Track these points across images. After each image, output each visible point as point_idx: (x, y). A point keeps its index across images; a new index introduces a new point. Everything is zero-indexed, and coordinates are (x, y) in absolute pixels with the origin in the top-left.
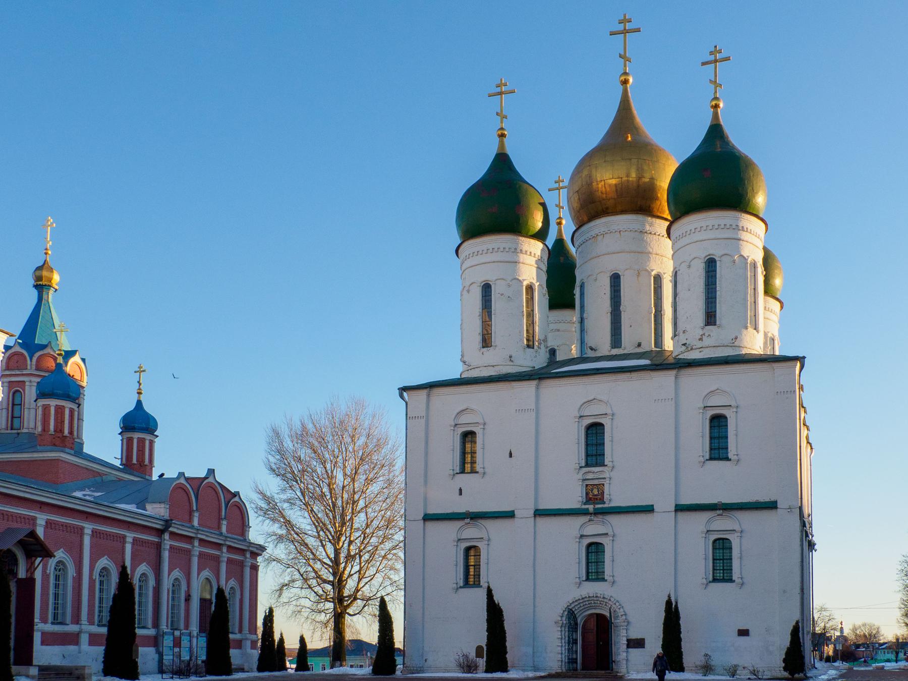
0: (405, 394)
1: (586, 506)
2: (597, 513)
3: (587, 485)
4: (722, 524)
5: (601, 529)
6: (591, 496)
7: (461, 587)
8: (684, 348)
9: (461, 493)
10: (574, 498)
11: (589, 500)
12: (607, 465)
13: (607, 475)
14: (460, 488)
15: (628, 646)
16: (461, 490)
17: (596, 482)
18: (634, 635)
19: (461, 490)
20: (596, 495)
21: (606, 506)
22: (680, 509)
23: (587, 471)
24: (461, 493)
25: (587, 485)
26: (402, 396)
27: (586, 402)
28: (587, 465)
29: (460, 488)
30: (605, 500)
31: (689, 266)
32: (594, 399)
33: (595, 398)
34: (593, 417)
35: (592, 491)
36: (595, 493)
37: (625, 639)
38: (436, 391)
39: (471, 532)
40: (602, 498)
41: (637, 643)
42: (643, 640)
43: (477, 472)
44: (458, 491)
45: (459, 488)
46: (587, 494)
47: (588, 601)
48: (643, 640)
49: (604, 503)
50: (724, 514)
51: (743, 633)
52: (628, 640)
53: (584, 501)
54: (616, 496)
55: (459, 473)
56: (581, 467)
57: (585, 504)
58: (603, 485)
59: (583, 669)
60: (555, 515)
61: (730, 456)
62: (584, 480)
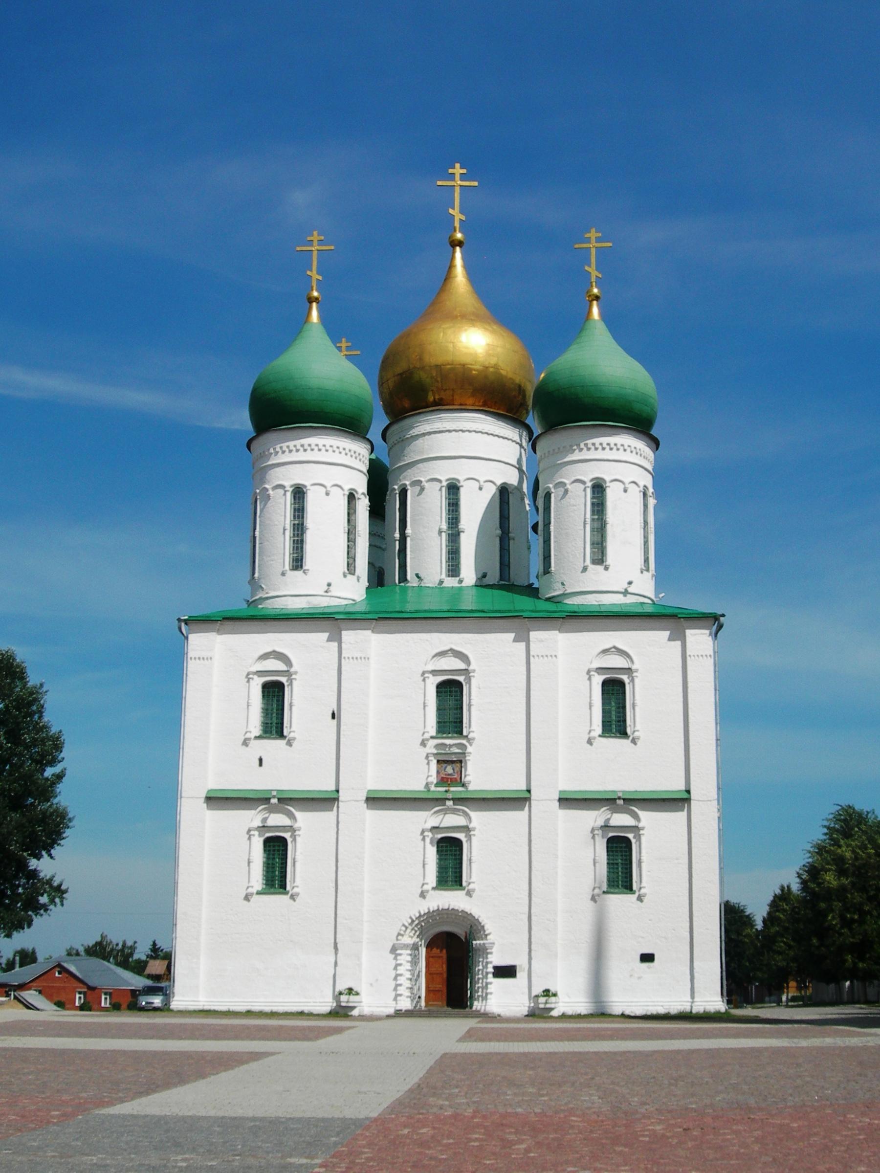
2: (457, 800)
3: (438, 761)
5: (460, 821)
6: (442, 776)
7: (258, 893)
9: (261, 764)
12: (467, 736)
13: (470, 749)
16: (261, 760)
19: (261, 760)
20: (449, 775)
24: (261, 764)
31: (566, 491)
35: (446, 767)
36: (450, 773)
39: (277, 819)
41: (506, 972)
44: (257, 762)
45: (258, 757)
46: (438, 772)
47: (439, 914)
50: (626, 806)
51: (647, 958)
52: (495, 968)
53: (435, 782)
56: (432, 737)
57: (437, 785)
58: (461, 762)
59: (426, 1006)
60: (395, 799)
61: (629, 731)
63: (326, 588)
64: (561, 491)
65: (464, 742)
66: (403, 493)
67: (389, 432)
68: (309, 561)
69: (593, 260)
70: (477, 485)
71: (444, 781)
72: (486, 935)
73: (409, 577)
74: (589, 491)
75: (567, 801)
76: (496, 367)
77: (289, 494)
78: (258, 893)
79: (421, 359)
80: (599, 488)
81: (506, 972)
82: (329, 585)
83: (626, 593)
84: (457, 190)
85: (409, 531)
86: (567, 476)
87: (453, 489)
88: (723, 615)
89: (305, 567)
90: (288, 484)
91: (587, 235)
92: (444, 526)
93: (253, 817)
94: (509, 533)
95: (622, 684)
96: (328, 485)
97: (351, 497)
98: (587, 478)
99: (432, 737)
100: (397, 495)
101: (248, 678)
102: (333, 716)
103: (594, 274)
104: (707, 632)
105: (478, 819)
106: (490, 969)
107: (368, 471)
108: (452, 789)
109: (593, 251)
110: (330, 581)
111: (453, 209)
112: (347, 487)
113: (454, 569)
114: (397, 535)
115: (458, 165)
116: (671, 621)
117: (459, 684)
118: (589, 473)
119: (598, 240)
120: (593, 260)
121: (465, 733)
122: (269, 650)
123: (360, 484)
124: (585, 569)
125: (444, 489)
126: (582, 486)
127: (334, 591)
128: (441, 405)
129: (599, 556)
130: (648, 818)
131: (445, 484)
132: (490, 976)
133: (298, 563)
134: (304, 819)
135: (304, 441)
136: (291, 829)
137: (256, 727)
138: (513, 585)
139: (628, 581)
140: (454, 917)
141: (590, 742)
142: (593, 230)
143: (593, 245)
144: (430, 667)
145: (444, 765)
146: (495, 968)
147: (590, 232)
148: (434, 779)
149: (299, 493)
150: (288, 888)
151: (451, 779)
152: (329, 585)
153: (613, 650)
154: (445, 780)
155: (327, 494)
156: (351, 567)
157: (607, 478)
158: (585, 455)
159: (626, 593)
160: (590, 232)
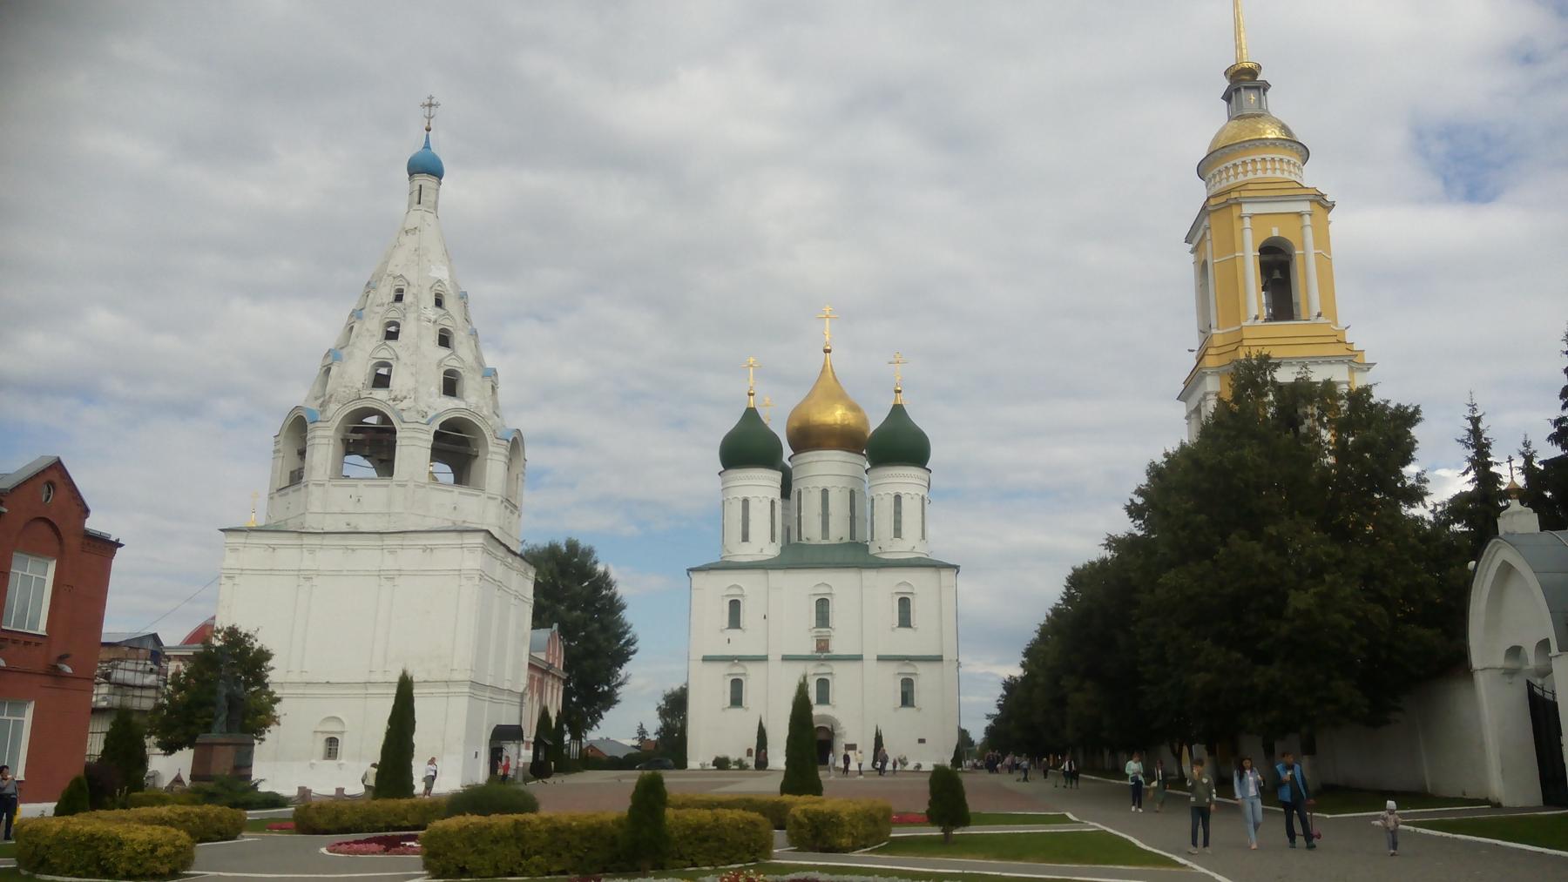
0: (690, 573)
4: (908, 669)
5: (826, 670)
8: (878, 550)
10: (809, 648)
11: (820, 649)
13: (832, 634)
16: (729, 640)
17: (825, 638)
18: (850, 741)
19: (729, 640)
22: (881, 659)
26: (688, 574)
28: (817, 626)
38: (712, 572)
39: (737, 670)
49: (829, 652)
51: (922, 741)
52: (846, 745)
54: (836, 648)
55: (729, 628)
58: (828, 640)
61: (912, 624)
64: (879, 497)
66: (800, 493)
67: (792, 459)
68: (751, 537)
73: (803, 539)
74: (893, 499)
75: (881, 659)
76: (848, 425)
80: (898, 498)
82: (762, 550)
83: (911, 551)
85: (802, 514)
87: (825, 492)
89: (750, 540)
90: (741, 497)
92: (821, 513)
93: (723, 668)
96: (761, 496)
97: (773, 502)
98: (893, 492)
101: (723, 599)
102: (765, 617)
104: (951, 573)
105: (837, 668)
106: (844, 746)
107: (781, 486)
108: (825, 654)
112: (770, 497)
114: (797, 516)
116: (933, 569)
118: (893, 491)
122: (732, 584)
123: (776, 494)
124: (892, 540)
126: (889, 496)
127: (765, 552)
128: (819, 446)
129: (898, 532)
130: (921, 668)
133: (745, 538)
134: (752, 670)
135: (747, 474)
136: (744, 674)
137: (726, 624)
138: (857, 543)
141: (893, 629)
144: (813, 593)
146: (846, 745)
149: (746, 502)
150: (743, 705)
152: (762, 550)
155: (760, 501)
156: (773, 539)
158: (890, 480)
159: (911, 551)
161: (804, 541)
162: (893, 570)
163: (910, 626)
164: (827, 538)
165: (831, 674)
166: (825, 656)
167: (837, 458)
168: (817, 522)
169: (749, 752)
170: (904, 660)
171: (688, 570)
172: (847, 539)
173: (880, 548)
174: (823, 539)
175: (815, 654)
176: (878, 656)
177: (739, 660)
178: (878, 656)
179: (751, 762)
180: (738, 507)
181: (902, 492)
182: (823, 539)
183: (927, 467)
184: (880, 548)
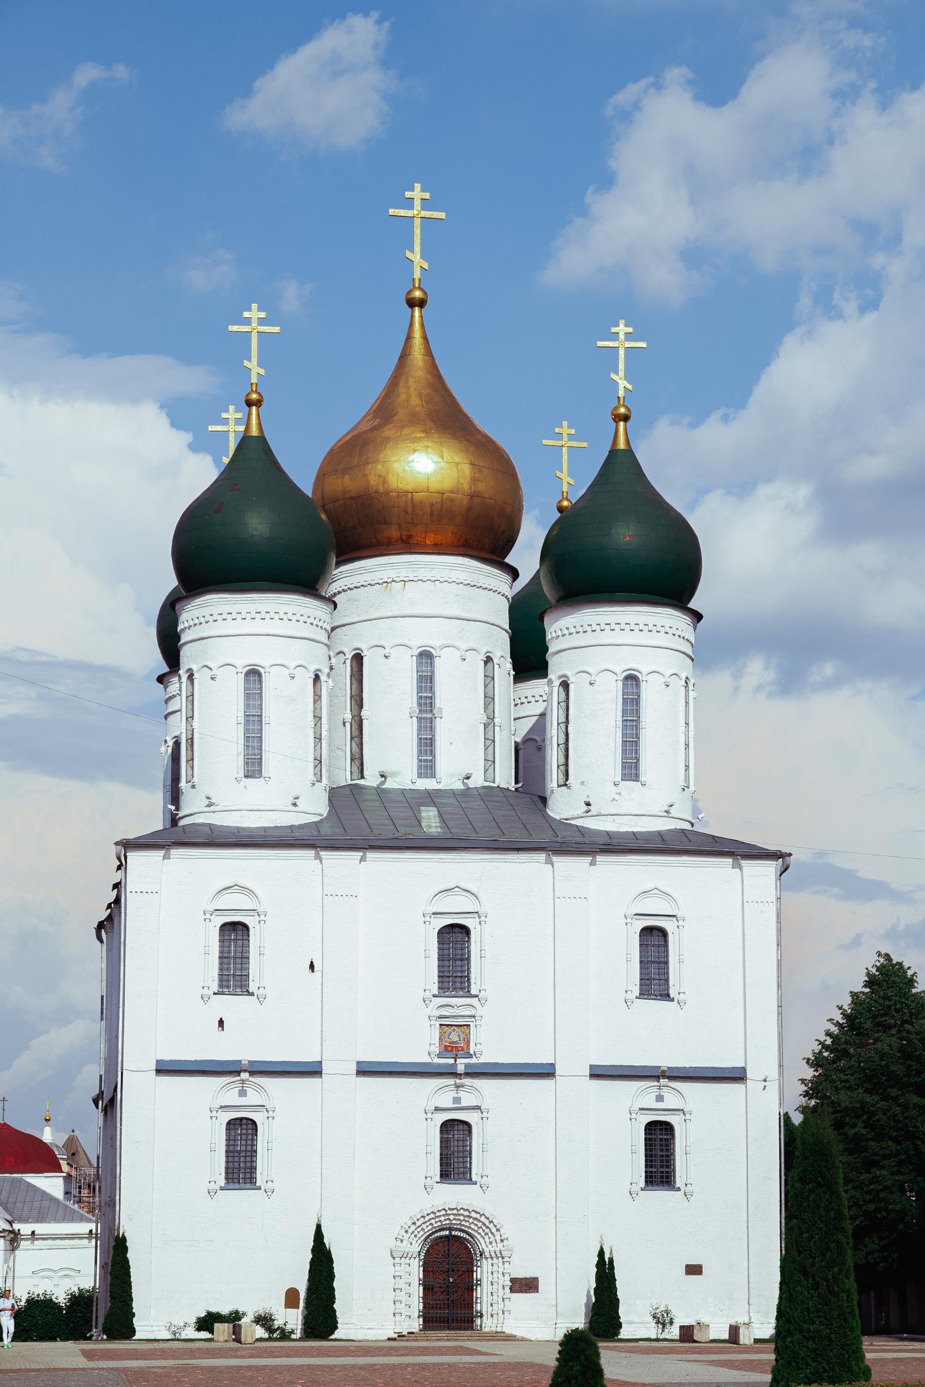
1: (442, 1061)
12: (477, 996)
13: (479, 1013)
14: (221, 1019)
15: (512, 1290)
16: (221, 1023)
17: (461, 1021)
19: (221, 1023)
20: (454, 1042)
21: (474, 1061)
22: (598, 1073)
23: (445, 1003)
25: (441, 1025)
27: (443, 891)
29: (221, 1019)
30: (472, 1052)
32: (457, 887)
33: (459, 886)
34: (455, 916)
37: (507, 1278)
40: (465, 1047)
41: (525, 1285)
42: (536, 1280)
43: (252, 994)
48: (536, 1280)
49: (470, 1056)
51: (694, 1270)
52: (513, 1280)
53: (438, 1053)
56: (434, 996)
60: (390, 1074)
61: (672, 993)
62: (439, 1018)
63: (291, 800)
65: (474, 1001)
69: (621, 366)
70: (458, 654)
71: (449, 1049)
72: (502, 1241)
74: (620, 684)
75: (598, 1073)
77: (242, 677)
78: (222, 1189)
79: (385, 482)
81: (525, 1285)
84: (417, 222)
86: (594, 661)
88: (790, 855)
91: (614, 330)
94: (494, 717)
95: (663, 933)
99: (434, 996)
100: (348, 662)
102: (312, 966)
103: (623, 384)
109: (622, 352)
110: (297, 793)
111: (412, 251)
112: (313, 668)
113: (427, 768)
114: (348, 716)
115: (418, 186)
117: (465, 930)
119: (629, 337)
120: (621, 366)
121: (473, 992)
125: (415, 658)
131: (416, 652)
132: (507, 1290)
139: (669, 802)
140: (462, 1218)
142: (622, 323)
143: (622, 346)
145: (446, 1028)
146: (512, 1280)
147: (618, 326)
148: (436, 1049)
151: (456, 1047)
153: (655, 892)
154: (450, 1049)
157: (645, 669)
160: (618, 326)
161: (371, 780)
162: (685, 858)
163: (666, 996)
164: (433, 776)
165: (478, 1108)
166: (467, 1065)
167: (462, 576)
168: (409, 733)
169: (291, 1298)
170: (658, 1078)
171: (117, 844)
172: (478, 781)
173: (588, 804)
174: (420, 776)
175: (437, 1061)
176: (591, 1067)
177: (252, 1073)
178: (591, 1067)
179: (293, 1319)
180: (236, 685)
181: (642, 665)
182: (420, 776)
183: (691, 605)
184: (588, 804)
